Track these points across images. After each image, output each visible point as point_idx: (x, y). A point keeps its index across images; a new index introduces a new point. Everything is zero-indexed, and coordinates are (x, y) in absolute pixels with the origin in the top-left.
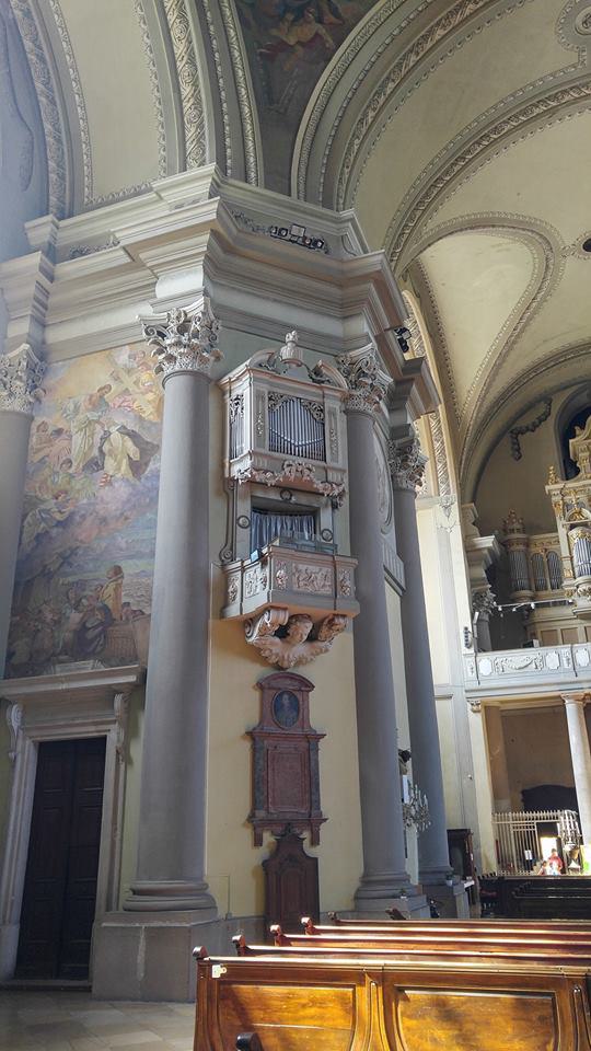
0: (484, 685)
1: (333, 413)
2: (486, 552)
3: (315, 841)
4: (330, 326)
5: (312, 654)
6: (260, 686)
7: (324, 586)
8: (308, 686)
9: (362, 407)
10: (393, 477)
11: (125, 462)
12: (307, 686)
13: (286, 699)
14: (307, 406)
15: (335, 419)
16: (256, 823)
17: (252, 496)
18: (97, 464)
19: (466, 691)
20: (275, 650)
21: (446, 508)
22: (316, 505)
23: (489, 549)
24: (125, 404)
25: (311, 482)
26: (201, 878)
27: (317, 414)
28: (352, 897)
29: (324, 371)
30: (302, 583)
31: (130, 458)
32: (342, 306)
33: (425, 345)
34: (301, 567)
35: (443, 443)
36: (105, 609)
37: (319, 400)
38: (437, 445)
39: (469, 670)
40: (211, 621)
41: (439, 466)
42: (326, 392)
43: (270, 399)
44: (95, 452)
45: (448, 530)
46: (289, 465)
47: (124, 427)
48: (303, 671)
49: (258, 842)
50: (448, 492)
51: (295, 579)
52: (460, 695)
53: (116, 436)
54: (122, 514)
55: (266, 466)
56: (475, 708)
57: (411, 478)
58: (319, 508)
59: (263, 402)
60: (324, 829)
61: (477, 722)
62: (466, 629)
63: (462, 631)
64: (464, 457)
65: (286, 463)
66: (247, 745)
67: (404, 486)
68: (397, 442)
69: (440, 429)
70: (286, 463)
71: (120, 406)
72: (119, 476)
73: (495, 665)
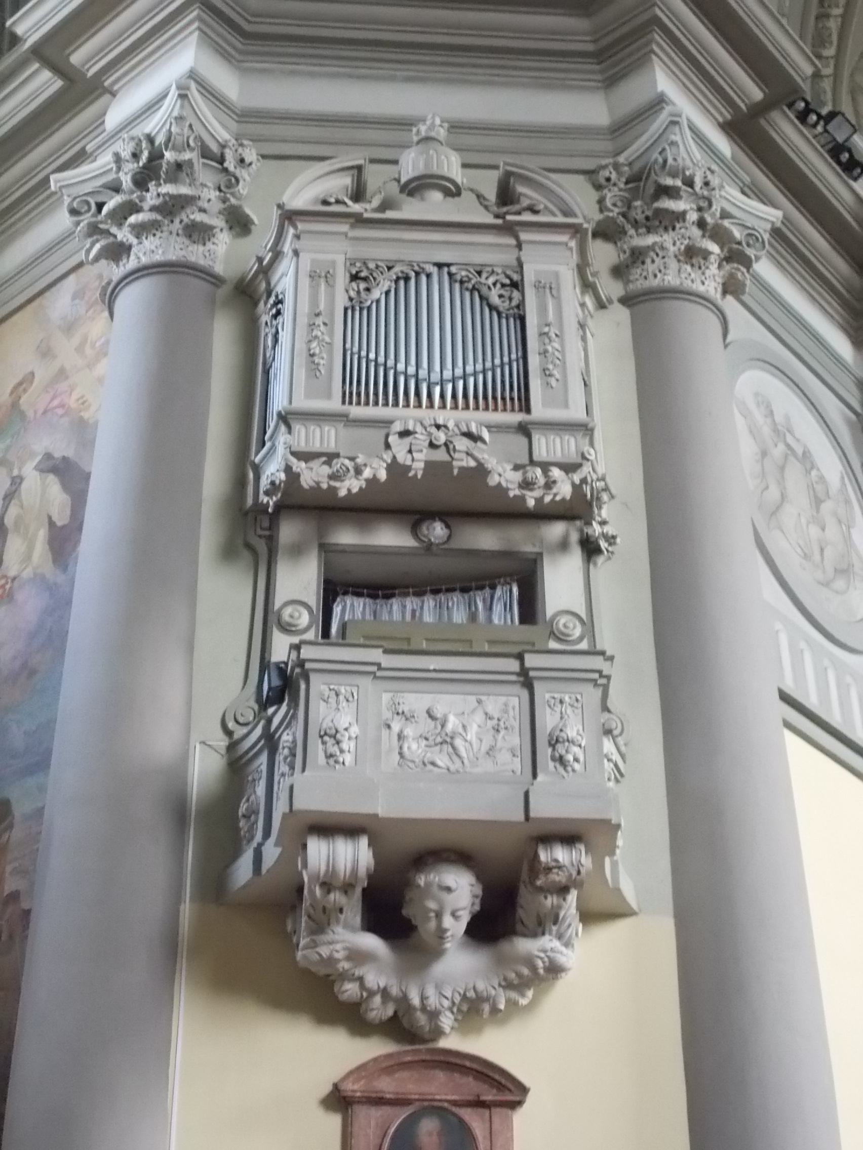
1: (549, 288)
5: (508, 985)
7: (491, 752)
9: (671, 279)
11: (42, 534)
13: (428, 1127)
15: (557, 299)
17: (325, 549)
20: (374, 978)
22: (529, 548)
24: (56, 403)
25: (481, 471)
29: (521, 189)
30: (414, 748)
31: (51, 523)
32: (599, 56)
37: (510, 258)
42: (523, 236)
43: (355, 277)
46: (405, 434)
47: (48, 456)
51: (388, 740)
54: (24, 665)
55: (331, 447)
59: (330, 284)
70: (398, 427)
71: (45, 412)
72: (27, 573)
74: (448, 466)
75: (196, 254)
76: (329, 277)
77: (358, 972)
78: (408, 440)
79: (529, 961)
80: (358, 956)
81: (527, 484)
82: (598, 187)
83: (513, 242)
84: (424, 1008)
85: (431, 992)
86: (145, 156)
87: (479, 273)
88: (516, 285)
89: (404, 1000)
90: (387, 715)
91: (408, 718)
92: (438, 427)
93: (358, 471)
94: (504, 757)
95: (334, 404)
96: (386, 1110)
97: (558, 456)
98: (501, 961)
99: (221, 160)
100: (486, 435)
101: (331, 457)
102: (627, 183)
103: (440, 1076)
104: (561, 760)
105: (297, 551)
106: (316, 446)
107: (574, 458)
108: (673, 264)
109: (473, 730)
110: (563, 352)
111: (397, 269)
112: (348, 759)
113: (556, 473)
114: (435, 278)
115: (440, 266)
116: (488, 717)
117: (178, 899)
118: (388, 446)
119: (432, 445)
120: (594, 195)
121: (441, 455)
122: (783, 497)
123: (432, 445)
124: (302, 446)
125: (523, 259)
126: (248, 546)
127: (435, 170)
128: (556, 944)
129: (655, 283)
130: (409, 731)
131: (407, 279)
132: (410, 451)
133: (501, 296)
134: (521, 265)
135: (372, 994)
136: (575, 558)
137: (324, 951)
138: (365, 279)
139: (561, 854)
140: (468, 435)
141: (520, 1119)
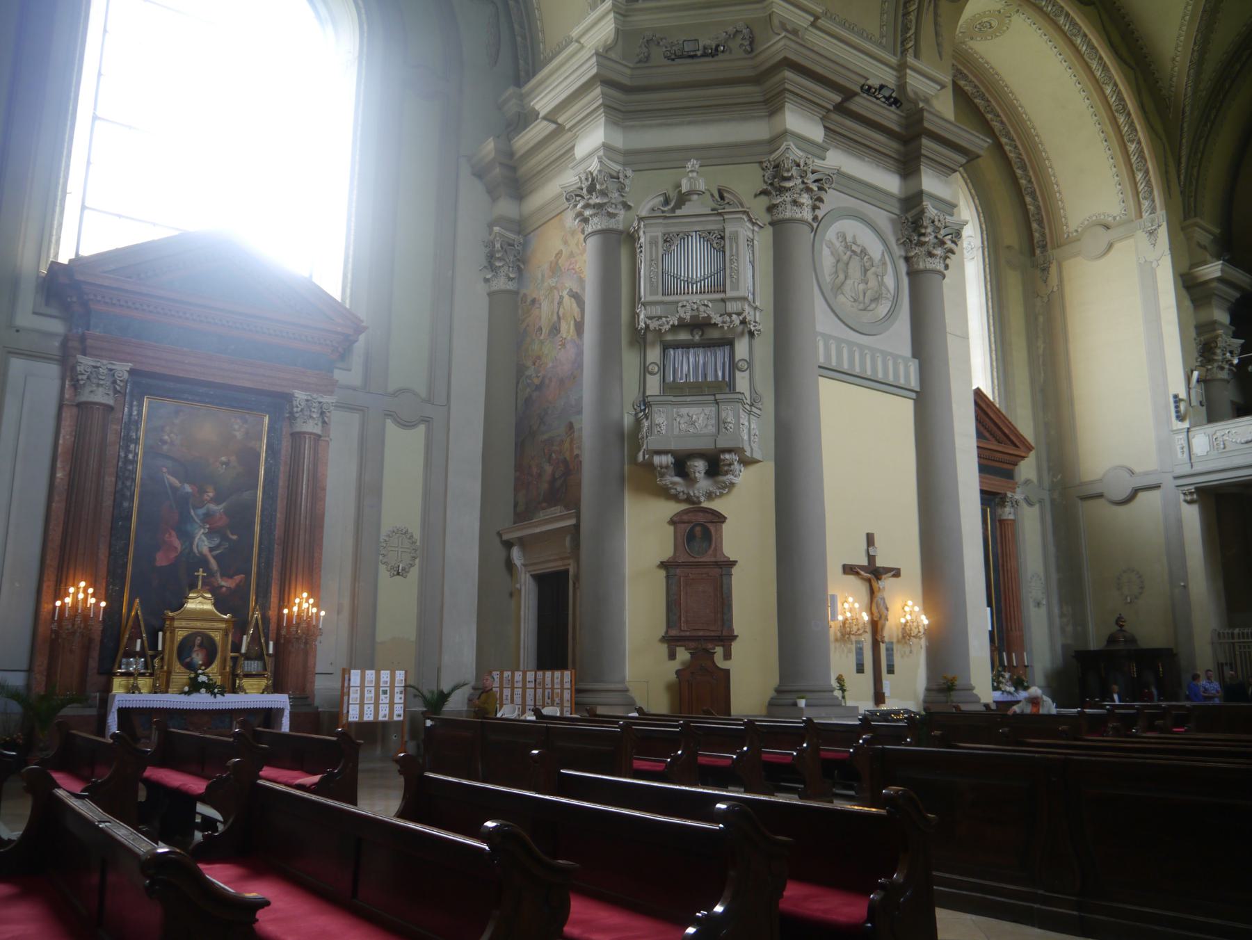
0: (1198, 468)
2: (1215, 284)
3: (727, 656)
4: (753, 130)
5: (719, 488)
6: (672, 522)
7: (706, 426)
8: (719, 518)
9: (788, 214)
10: (907, 259)
11: (572, 322)
12: (719, 518)
13: (698, 529)
14: (706, 236)
15: (737, 243)
16: (671, 642)
17: (661, 341)
18: (556, 329)
19: (1176, 478)
20: (679, 489)
21: (1151, 233)
23: (1219, 279)
24: (571, 267)
25: (709, 317)
26: (623, 681)
27: (718, 241)
28: (766, 703)
32: (766, 102)
33: (1078, 20)
34: (684, 411)
35: (1139, 143)
36: (565, 461)
37: (719, 226)
38: (1132, 147)
39: (1179, 451)
40: (626, 467)
41: (1139, 176)
42: (726, 217)
43: (665, 241)
44: (555, 317)
45: (1154, 265)
46: (683, 306)
48: (716, 505)
49: (672, 656)
50: (1153, 211)
52: (1169, 483)
53: (567, 299)
55: (659, 313)
56: (1189, 498)
57: (931, 255)
58: (734, 338)
59: (657, 247)
60: (735, 646)
61: (1192, 516)
62: (1176, 396)
63: (1172, 400)
64: (1184, 152)
65: (680, 304)
66: (662, 573)
67: (921, 266)
68: (909, 215)
69: (1132, 125)
70: (680, 304)
71: (568, 270)
72: (569, 338)
73: (1213, 443)
74: (698, 316)
75: (612, 224)
76: (656, 243)
77: (675, 487)
78: (684, 309)
79: (724, 482)
80: (674, 483)
81: (724, 322)
82: (763, 169)
83: (722, 218)
84: (695, 496)
85: (696, 492)
86: (590, 180)
87: (709, 233)
88: (723, 238)
89: (688, 494)
90: (675, 416)
91: (681, 416)
92: (694, 303)
93: (668, 323)
94: (710, 427)
95: (659, 298)
96: (686, 525)
97: (735, 310)
98: (716, 482)
99: (618, 178)
100: (710, 305)
101: (660, 318)
102: (774, 168)
103: (701, 514)
104: (726, 428)
105: (653, 344)
106: (654, 314)
107: (740, 310)
108: (789, 206)
109: (701, 419)
110: (738, 267)
111: (681, 235)
112: (664, 432)
113: (734, 317)
114: (694, 237)
115: (696, 232)
116: (705, 415)
117: (623, 464)
118: (678, 312)
119: (692, 309)
120: (762, 173)
121: (695, 313)
122: (846, 278)
123: (692, 309)
124: (649, 314)
125: (726, 227)
126: (638, 342)
127: (693, 189)
128: (732, 477)
129: (781, 216)
130: (681, 422)
131: (684, 239)
132: (685, 313)
133: (717, 243)
134: (724, 229)
135: (679, 493)
136: (746, 339)
137: (664, 482)
138: (669, 241)
139: (727, 456)
140: (704, 305)
141: (724, 526)
